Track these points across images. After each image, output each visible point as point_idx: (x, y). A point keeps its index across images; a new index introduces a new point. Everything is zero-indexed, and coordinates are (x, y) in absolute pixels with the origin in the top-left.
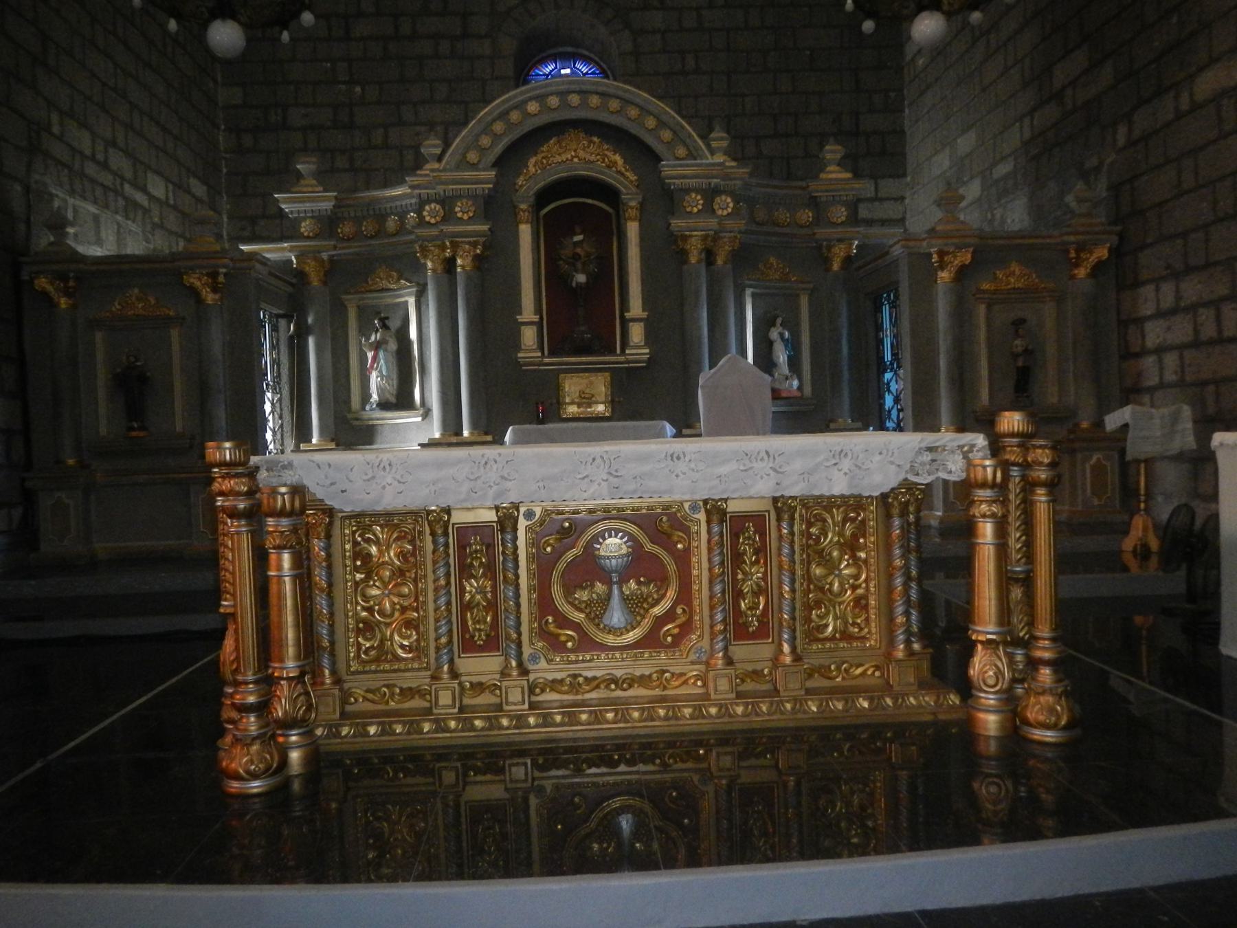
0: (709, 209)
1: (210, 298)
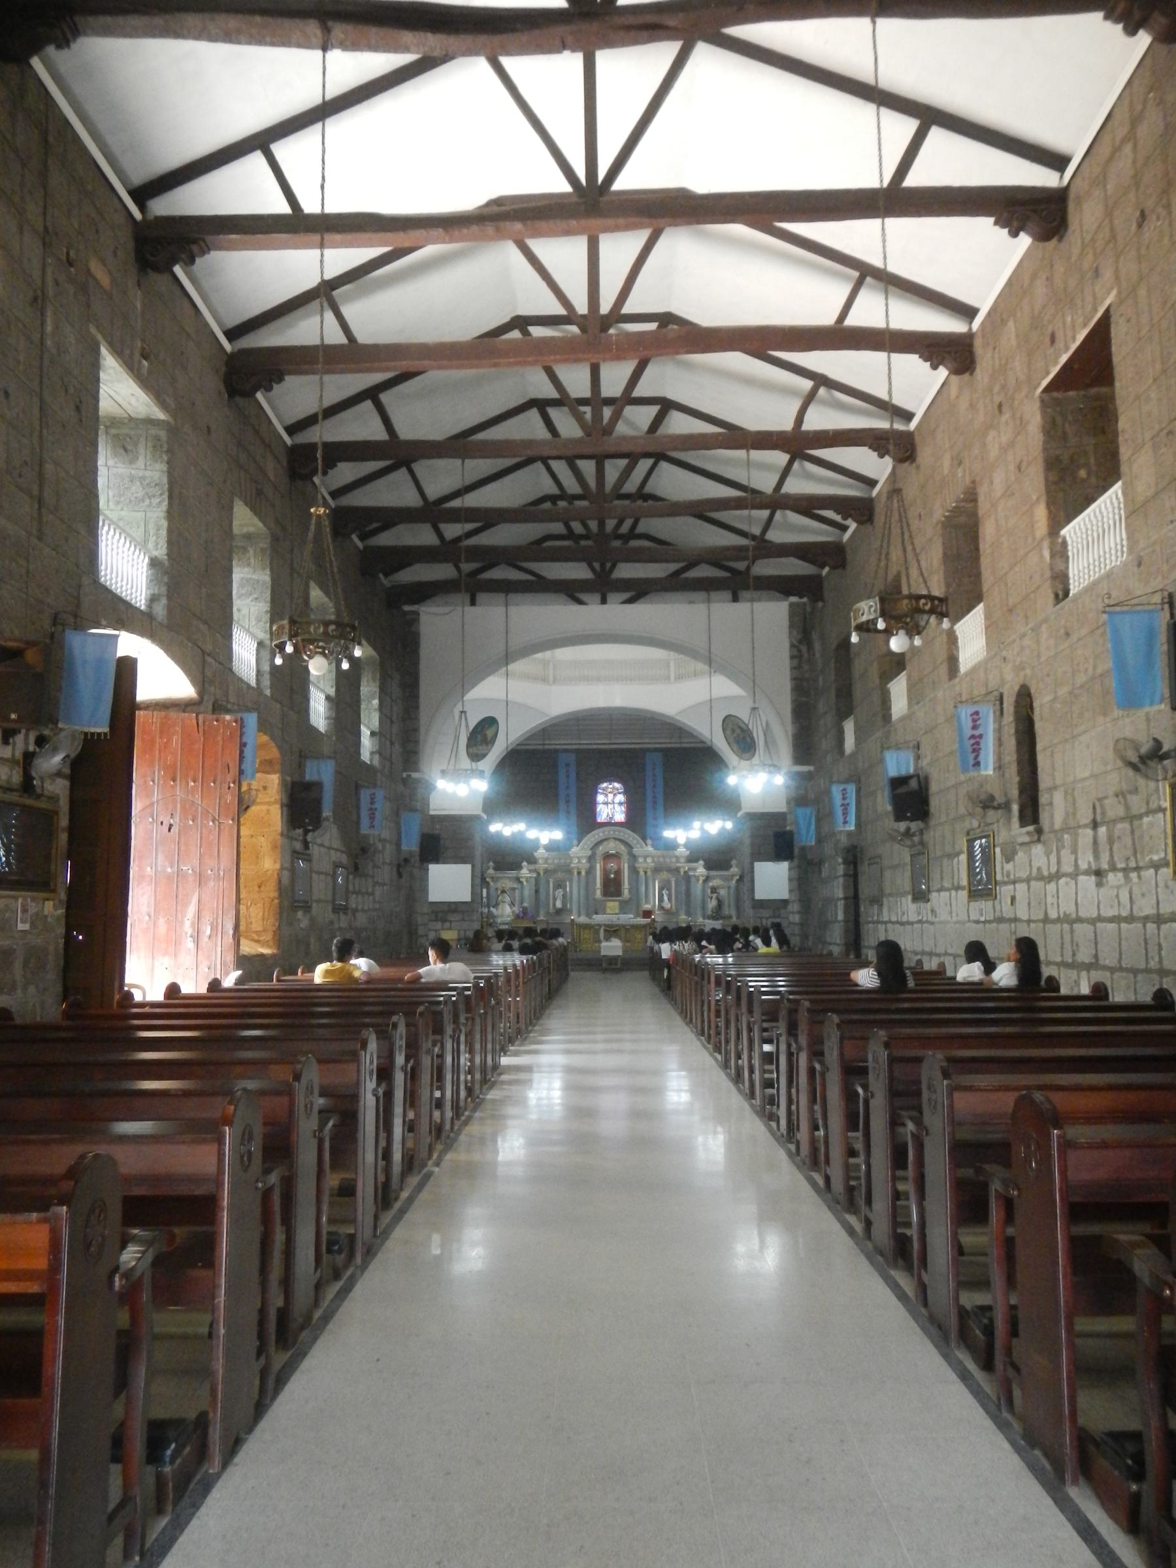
0: (645, 860)
1: (525, 883)
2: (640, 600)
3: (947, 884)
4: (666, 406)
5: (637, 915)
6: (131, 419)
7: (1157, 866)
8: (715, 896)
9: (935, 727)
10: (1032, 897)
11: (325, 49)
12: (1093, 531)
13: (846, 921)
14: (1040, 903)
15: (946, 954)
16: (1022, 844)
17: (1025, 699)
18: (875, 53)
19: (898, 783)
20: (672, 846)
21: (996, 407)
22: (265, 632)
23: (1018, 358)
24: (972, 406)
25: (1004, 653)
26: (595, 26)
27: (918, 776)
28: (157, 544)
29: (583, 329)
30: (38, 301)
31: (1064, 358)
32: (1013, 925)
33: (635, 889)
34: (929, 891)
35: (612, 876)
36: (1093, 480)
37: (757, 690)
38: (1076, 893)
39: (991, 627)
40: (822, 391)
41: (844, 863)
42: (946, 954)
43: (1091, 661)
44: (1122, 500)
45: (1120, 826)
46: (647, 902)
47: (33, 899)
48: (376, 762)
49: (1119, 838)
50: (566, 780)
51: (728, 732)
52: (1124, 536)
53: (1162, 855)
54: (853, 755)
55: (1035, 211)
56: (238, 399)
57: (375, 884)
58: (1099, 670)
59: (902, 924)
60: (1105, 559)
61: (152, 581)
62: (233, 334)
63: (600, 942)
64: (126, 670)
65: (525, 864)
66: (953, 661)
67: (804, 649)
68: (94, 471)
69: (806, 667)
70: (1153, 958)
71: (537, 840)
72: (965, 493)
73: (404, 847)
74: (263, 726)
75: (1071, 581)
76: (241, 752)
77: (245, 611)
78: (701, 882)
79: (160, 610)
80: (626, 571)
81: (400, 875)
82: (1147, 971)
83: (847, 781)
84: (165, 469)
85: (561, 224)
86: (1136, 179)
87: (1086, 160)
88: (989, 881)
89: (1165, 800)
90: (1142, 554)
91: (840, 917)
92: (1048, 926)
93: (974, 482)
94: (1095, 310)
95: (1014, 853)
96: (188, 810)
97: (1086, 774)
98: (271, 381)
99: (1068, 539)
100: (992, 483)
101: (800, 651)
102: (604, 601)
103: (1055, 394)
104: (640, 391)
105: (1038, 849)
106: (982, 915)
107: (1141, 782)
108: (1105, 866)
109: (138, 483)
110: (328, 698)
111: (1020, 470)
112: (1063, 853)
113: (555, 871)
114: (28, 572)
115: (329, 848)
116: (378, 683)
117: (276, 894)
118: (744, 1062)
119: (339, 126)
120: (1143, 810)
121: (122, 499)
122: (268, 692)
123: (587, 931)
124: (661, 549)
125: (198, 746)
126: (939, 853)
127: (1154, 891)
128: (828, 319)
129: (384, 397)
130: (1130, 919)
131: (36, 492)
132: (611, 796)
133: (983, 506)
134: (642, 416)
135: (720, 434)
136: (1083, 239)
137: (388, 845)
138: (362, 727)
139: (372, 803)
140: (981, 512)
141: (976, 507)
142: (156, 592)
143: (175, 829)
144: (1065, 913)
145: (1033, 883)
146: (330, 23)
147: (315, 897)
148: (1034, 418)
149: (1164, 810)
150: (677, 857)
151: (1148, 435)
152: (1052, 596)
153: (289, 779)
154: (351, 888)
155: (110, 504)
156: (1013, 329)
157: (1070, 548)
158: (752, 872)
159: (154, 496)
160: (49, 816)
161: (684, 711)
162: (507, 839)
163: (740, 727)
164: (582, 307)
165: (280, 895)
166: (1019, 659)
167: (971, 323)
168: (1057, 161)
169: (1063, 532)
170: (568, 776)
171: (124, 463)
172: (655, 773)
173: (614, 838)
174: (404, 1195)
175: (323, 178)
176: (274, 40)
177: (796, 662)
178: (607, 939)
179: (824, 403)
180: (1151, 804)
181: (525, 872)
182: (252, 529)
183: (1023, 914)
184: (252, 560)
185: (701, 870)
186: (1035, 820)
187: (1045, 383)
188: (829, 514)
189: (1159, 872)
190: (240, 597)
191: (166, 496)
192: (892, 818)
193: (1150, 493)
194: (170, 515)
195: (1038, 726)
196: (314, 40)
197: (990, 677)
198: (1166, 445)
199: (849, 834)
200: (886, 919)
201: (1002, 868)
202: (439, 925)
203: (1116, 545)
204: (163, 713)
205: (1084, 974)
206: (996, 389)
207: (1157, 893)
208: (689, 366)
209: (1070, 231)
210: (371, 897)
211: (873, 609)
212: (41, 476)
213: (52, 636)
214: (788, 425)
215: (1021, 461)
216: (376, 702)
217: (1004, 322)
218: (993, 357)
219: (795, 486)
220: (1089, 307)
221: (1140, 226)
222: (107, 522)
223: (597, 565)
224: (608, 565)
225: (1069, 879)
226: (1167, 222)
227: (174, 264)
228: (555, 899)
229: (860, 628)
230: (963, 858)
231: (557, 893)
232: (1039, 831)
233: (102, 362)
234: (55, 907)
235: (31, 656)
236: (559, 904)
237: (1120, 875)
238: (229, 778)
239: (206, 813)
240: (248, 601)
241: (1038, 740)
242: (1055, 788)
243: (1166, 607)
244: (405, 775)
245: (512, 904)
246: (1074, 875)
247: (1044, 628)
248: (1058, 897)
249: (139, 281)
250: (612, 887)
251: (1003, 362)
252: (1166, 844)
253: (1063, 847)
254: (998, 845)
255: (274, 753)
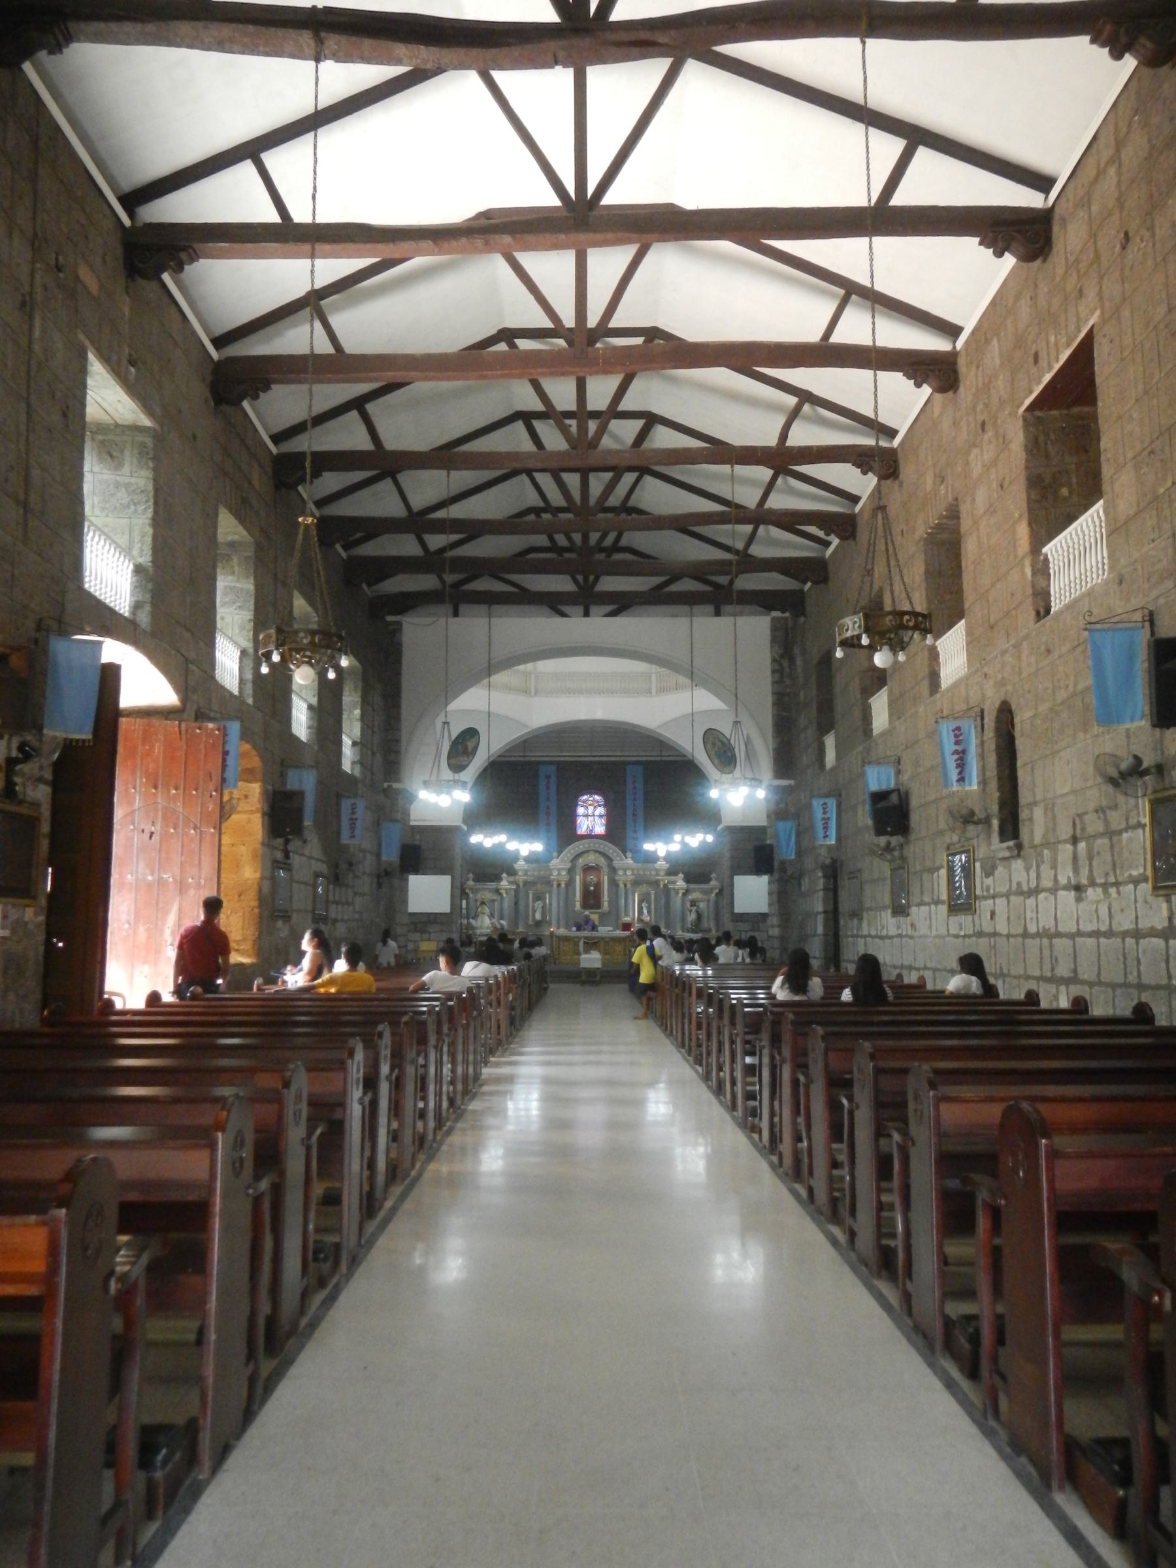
0: (625, 874)
2: (624, 613)
3: (926, 899)
4: (651, 420)
5: (616, 928)
6: (117, 425)
7: (1136, 882)
8: (694, 909)
9: (917, 741)
10: (1012, 912)
11: (318, 60)
12: (1074, 549)
13: (825, 935)
14: (1019, 918)
15: (925, 968)
16: (1004, 859)
17: (1006, 714)
18: (865, 73)
19: (879, 797)
20: (652, 858)
21: (979, 427)
22: (248, 641)
23: (1001, 377)
24: (955, 424)
25: (986, 669)
26: (587, 42)
27: (899, 790)
28: (142, 550)
29: (570, 343)
30: (26, 306)
31: (1047, 378)
32: (992, 940)
33: (614, 902)
34: (909, 905)
35: (592, 888)
36: (1075, 499)
37: (739, 703)
38: (1056, 908)
39: (973, 643)
40: (806, 407)
41: (824, 876)
42: (925, 968)
43: (1072, 678)
44: (1103, 518)
45: (1099, 841)
46: (627, 915)
47: (14, 905)
48: (357, 772)
49: (1098, 853)
50: (547, 793)
51: (709, 746)
52: (1105, 554)
53: (1142, 871)
54: (832, 769)
55: (1019, 232)
56: (225, 408)
57: (355, 894)
58: (1080, 687)
59: (882, 938)
60: (1087, 577)
61: (136, 587)
62: (220, 342)
63: (579, 954)
64: (110, 676)
65: (504, 875)
66: (934, 677)
67: (785, 663)
68: (79, 477)
69: (788, 682)
70: (1131, 973)
71: (517, 852)
72: (946, 510)
73: (384, 858)
74: (245, 736)
75: (1052, 599)
76: (224, 760)
77: (228, 619)
78: (680, 895)
79: (144, 619)
80: (610, 584)
81: (380, 885)
82: (1126, 985)
83: (827, 796)
84: (151, 476)
85: (549, 238)
86: (1120, 203)
87: (1072, 185)
88: (969, 895)
89: (1145, 817)
90: (1123, 572)
91: (820, 930)
92: (1028, 941)
93: (956, 499)
94: (1080, 331)
95: (994, 867)
96: (169, 817)
97: (1066, 790)
98: (257, 389)
99: (1049, 556)
100: (974, 500)
101: (781, 665)
102: (586, 614)
103: (1038, 413)
104: (625, 405)
105: (1018, 864)
106: (961, 929)
107: (1121, 799)
108: (1085, 881)
109: (124, 490)
110: (310, 707)
111: (1002, 487)
112: (1042, 867)
113: (534, 883)
114: (13, 576)
115: (311, 858)
116: (359, 693)
117: (255, 903)
118: (726, 1074)
119: (332, 137)
120: (1123, 825)
121: (107, 505)
122: (250, 701)
123: (566, 943)
124: (643, 563)
125: (181, 754)
126: (918, 867)
127: (1133, 907)
128: (812, 334)
129: (370, 407)
130: (1109, 934)
131: (22, 496)
132: (591, 809)
133: (966, 524)
134: (627, 430)
135: (704, 449)
136: (1066, 258)
137: (368, 856)
138: (344, 737)
139: (353, 813)
140: (963, 529)
141: (959, 524)
142: (140, 598)
143: (156, 837)
144: (1044, 927)
145: (1012, 898)
146: (323, 34)
147: (296, 905)
148: (1017, 438)
149: (1143, 826)
150: (657, 871)
151: (1130, 455)
152: (1033, 613)
153: (270, 788)
154: (331, 898)
155: (96, 510)
156: (996, 349)
157: (1051, 565)
158: (732, 885)
159: (139, 503)
160: (32, 822)
161: (666, 724)
162: (486, 851)
163: (721, 741)
164: (569, 321)
165: (260, 906)
166: (1000, 676)
167: (954, 342)
168: (1042, 182)
169: (1044, 550)
170: (548, 788)
171: (109, 470)
172: (635, 784)
173: (596, 851)
174: (388, 1204)
175: (315, 188)
176: (267, 49)
177: (777, 676)
178: (587, 951)
179: (808, 419)
180: (1130, 820)
181: (504, 884)
182: (236, 538)
183: (1002, 927)
184: (236, 568)
185: (680, 883)
186: (1015, 835)
187: (1028, 402)
188: (812, 530)
189: (1138, 887)
190: (224, 604)
191: (151, 503)
192: (872, 832)
193: (1132, 512)
194: (155, 522)
195: (1018, 742)
196: (306, 50)
197: (971, 694)
198: (1147, 464)
199: (830, 848)
200: (865, 932)
201: (981, 882)
202: (417, 936)
203: (1097, 562)
204: (145, 721)
205: (1063, 988)
206: (980, 407)
207: (1136, 908)
208: (674, 380)
209: (1055, 250)
210: (351, 908)
211: (857, 625)
212: (27, 479)
213: (36, 641)
214: (772, 441)
215: (1004, 479)
216: (357, 712)
217: (987, 341)
218: (977, 376)
219: (777, 502)
220: (1072, 328)
221: (1124, 248)
222: (92, 528)
223: (580, 578)
224: (592, 578)
225: (1048, 894)
226: (1151, 244)
227: (163, 272)
228: (534, 911)
229: (845, 644)
230: (943, 872)
231: (536, 905)
232: (1019, 847)
233: (89, 368)
234: (36, 914)
235: (15, 661)
236: (538, 916)
237: (1099, 890)
238: (211, 786)
239: (187, 820)
240: (232, 609)
241: (1018, 755)
242: (1035, 803)
243: (1147, 624)
244: (386, 785)
245: (492, 916)
246: (1054, 891)
247: (1025, 645)
248: (1037, 912)
249: (127, 287)
250: (591, 898)
251: (986, 380)
252: (1145, 859)
253: (1043, 862)
254: (978, 860)
255: (255, 762)
